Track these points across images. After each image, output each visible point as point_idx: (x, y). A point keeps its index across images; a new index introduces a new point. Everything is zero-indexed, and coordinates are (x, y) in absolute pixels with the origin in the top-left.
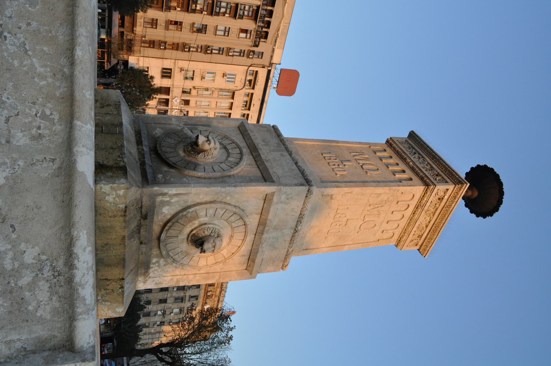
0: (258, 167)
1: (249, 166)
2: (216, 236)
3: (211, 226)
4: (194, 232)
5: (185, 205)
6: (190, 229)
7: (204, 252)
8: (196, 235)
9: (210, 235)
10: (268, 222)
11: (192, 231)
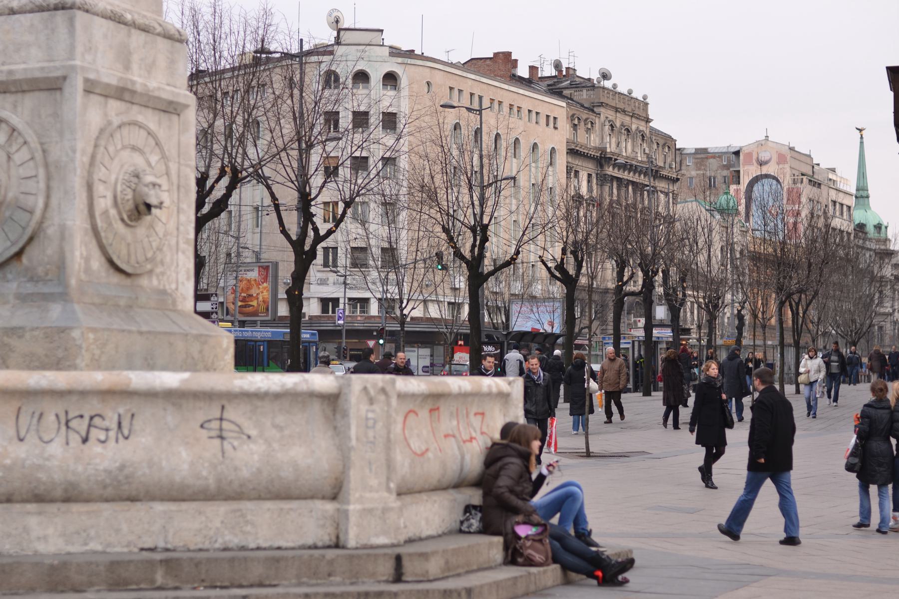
0: (23, 91)
1: (19, 109)
2: (135, 180)
3: (119, 188)
4: (125, 217)
5: (90, 233)
6: (119, 222)
7: (161, 203)
8: (129, 213)
9: (134, 191)
10: (121, 85)
11: (122, 220)
